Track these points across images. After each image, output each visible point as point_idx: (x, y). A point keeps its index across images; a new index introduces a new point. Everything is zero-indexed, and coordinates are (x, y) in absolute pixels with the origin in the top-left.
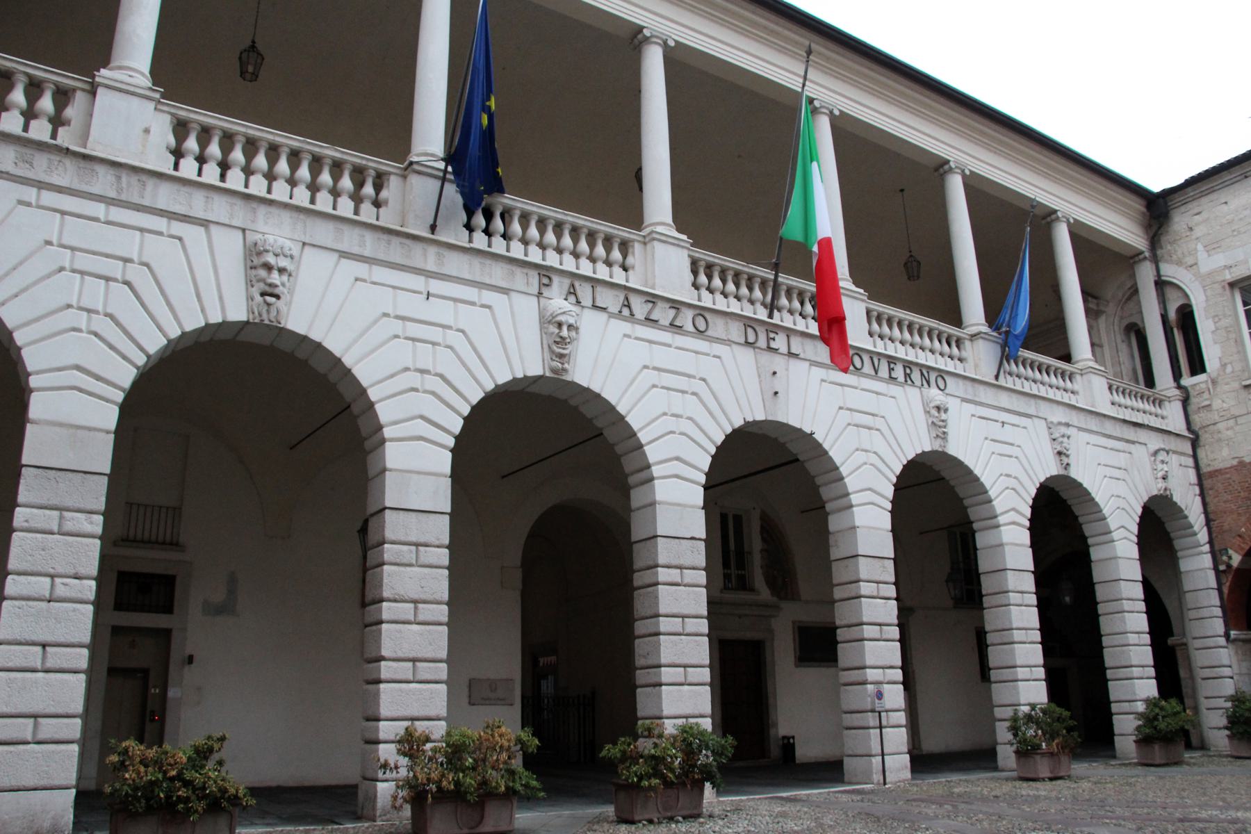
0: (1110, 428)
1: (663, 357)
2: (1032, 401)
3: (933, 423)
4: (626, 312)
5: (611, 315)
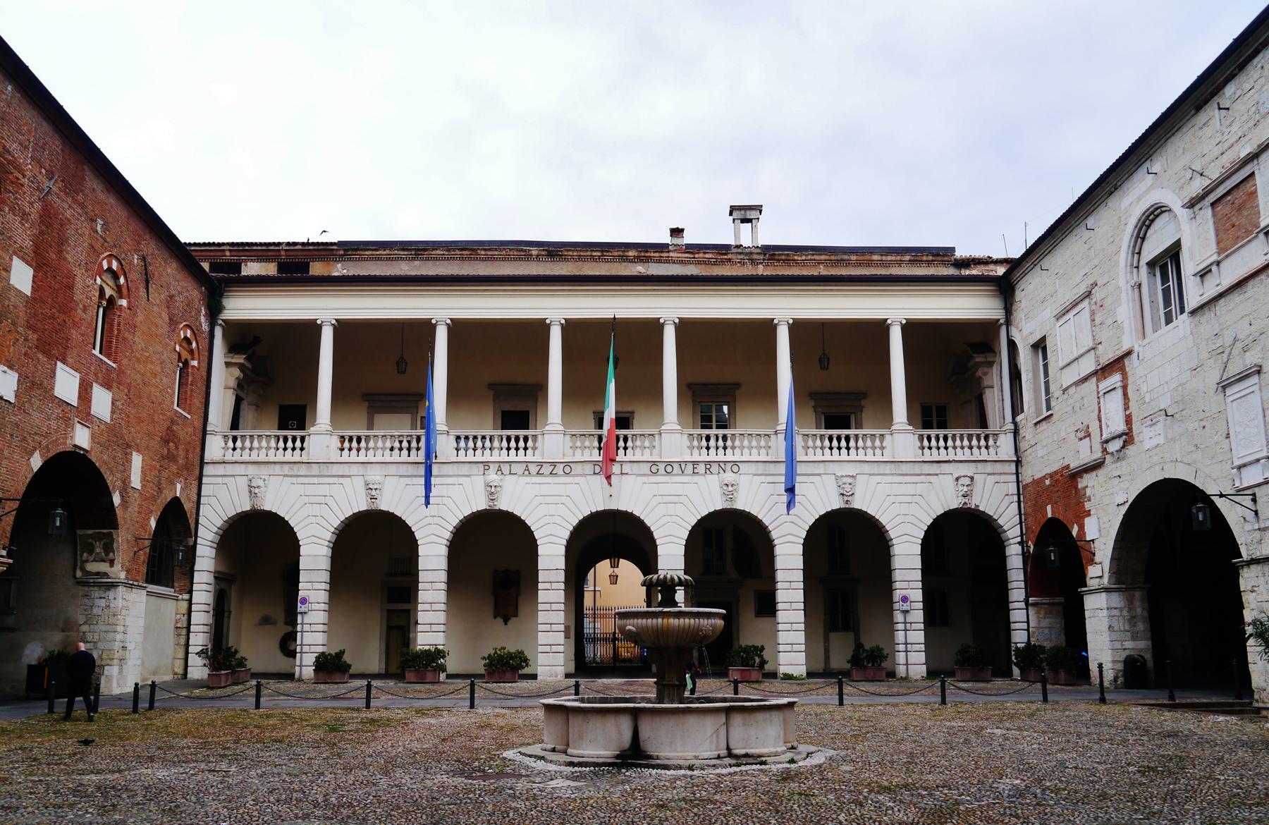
0: (917, 469)
1: (546, 489)
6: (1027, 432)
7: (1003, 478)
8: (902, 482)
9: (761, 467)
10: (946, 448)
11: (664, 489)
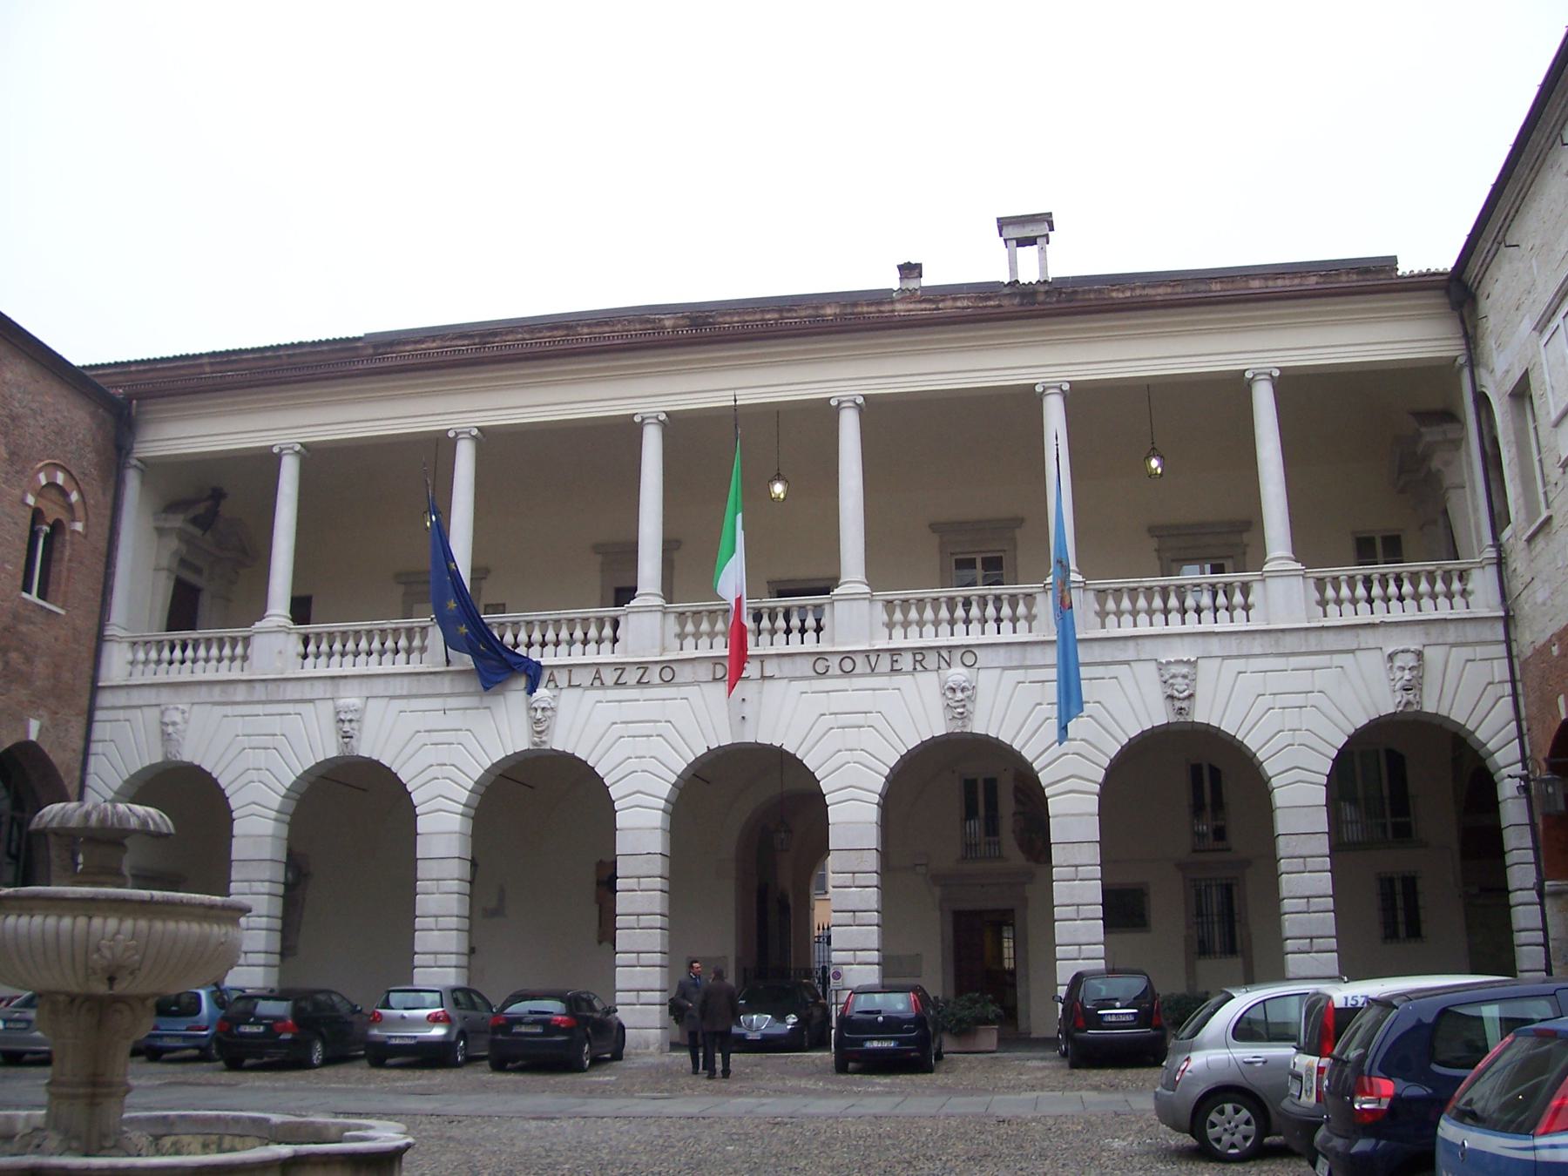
0: (1313, 642)
1: (629, 711)
2: (1131, 644)
4: (597, 683)
5: (586, 689)
6: (1518, 562)
7: (1480, 651)
8: (1291, 675)
9: (1016, 656)
10: (1370, 601)
11: (838, 702)
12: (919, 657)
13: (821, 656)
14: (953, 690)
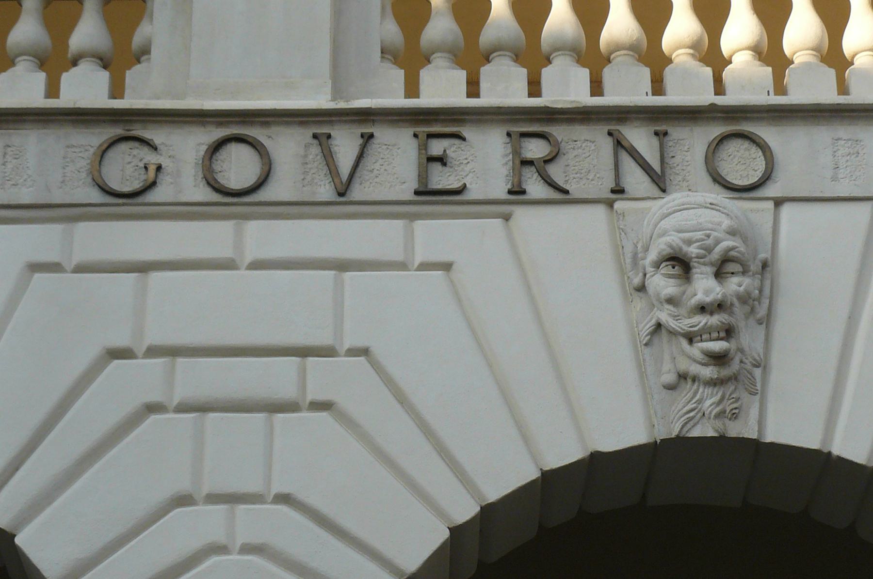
3: (659, 326)
11: (180, 307)
12: (535, 149)
13: (127, 126)
14: (680, 263)
